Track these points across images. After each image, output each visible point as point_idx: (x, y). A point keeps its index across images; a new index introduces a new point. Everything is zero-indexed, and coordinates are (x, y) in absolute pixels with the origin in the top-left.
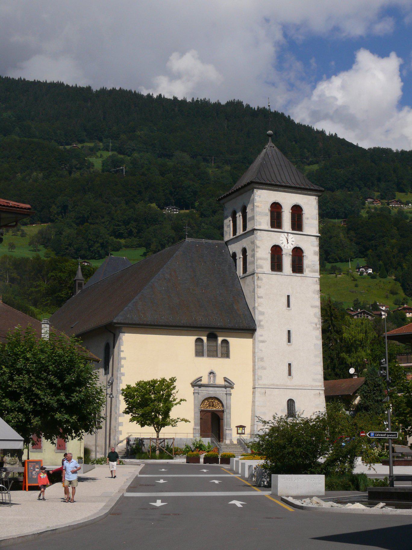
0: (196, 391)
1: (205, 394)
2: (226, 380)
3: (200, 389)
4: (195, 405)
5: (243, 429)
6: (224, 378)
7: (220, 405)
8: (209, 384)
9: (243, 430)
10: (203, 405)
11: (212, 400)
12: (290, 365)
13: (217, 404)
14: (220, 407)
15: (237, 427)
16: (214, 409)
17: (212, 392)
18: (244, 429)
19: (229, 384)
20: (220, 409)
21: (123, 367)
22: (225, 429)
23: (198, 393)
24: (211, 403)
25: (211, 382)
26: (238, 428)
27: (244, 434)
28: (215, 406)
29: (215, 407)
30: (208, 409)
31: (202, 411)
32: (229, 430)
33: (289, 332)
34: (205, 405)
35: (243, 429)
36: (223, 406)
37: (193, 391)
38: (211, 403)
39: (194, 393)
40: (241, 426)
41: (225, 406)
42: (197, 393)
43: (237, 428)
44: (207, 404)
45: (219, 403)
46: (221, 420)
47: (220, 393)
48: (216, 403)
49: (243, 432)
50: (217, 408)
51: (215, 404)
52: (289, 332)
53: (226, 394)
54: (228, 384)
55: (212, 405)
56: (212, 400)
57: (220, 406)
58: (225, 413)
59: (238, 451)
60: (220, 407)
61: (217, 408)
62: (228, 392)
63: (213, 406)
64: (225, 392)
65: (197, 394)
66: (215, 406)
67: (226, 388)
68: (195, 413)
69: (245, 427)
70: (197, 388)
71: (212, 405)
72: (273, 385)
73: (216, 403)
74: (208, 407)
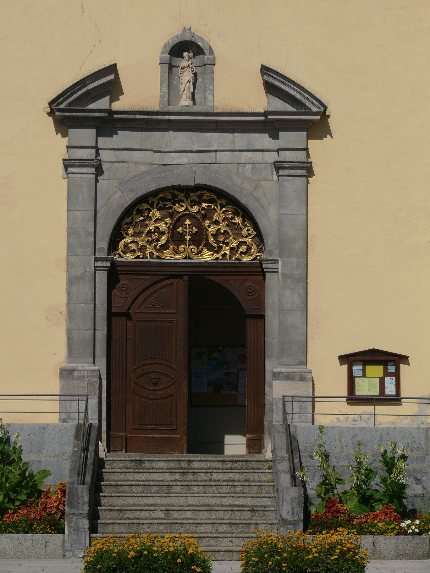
1: (143, 168)
3: (103, 142)
4: (71, 232)
5: (386, 374)
6: (265, 70)
7: (244, 232)
8: (171, 109)
9: (390, 383)
10: (137, 234)
11: (194, 203)
13: (223, 227)
14: (243, 248)
15: (347, 359)
16: (207, 256)
17: (183, 159)
18: (397, 375)
19: (293, 109)
20: (246, 259)
22: (268, 376)
24: (188, 222)
25: (185, 101)
26: (357, 369)
27: (396, 400)
28: (211, 239)
29: (210, 247)
30: (168, 256)
32: (288, 377)
34: (149, 233)
35: (386, 374)
36: (259, 238)
37: (63, 153)
38: (188, 222)
39: (67, 164)
40: (374, 352)
41: (270, 240)
42: (82, 163)
43: (350, 371)
44: (163, 227)
45: (238, 220)
46: (250, 324)
48: (217, 223)
49: (390, 390)
50: (226, 250)
51: (213, 229)
53: (278, 166)
54: (289, 108)
55: (193, 235)
56: (195, 209)
57: (248, 240)
58: (271, 280)
59: (210, 509)
60: (243, 248)
61: (226, 250)
62: (287, 156)
64: (271, 157)
65: (84, 170)
66: (211, 239)
67: (275, 136)
68: (71, 282)
69: (403, 359)
71: (193, 235)
73: (217, 223)
74: (165, 247)
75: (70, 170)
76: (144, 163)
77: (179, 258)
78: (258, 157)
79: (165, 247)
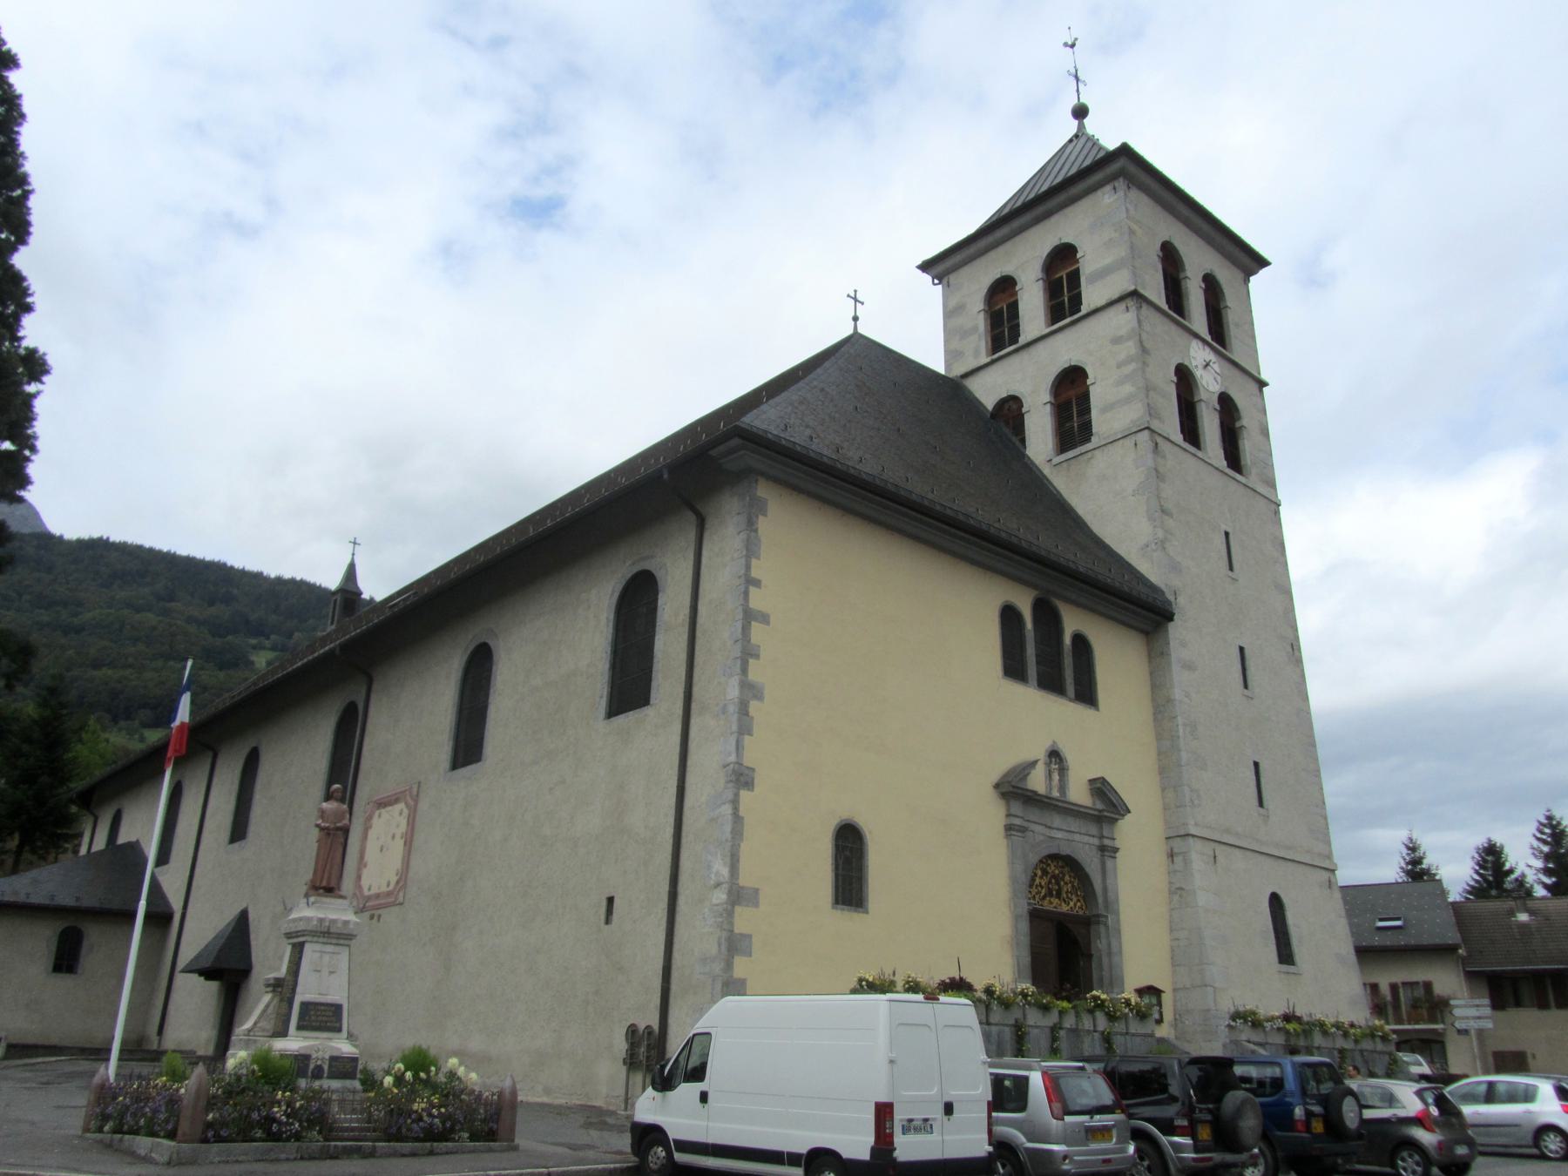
0: (1017, 821)
2: (1100, 788)
12: (1256, 765)
16: (1065, 908)
20: (1081, 913)
21: (757, 657)
23: (1023, 830)
31: (1036, 916)
33: (1242, 649)
39: (1009, 828)
47: (1079, 842)
52: (1242, 649)
63: (1059, 895)
64: (1096, 841)
70: (1017, 808)
72: (1227, 831)
75: (1009, 833)
76: (1043, 835)
77: (1051, 908)
78: (1086, 839)
79: (1044, 898)
